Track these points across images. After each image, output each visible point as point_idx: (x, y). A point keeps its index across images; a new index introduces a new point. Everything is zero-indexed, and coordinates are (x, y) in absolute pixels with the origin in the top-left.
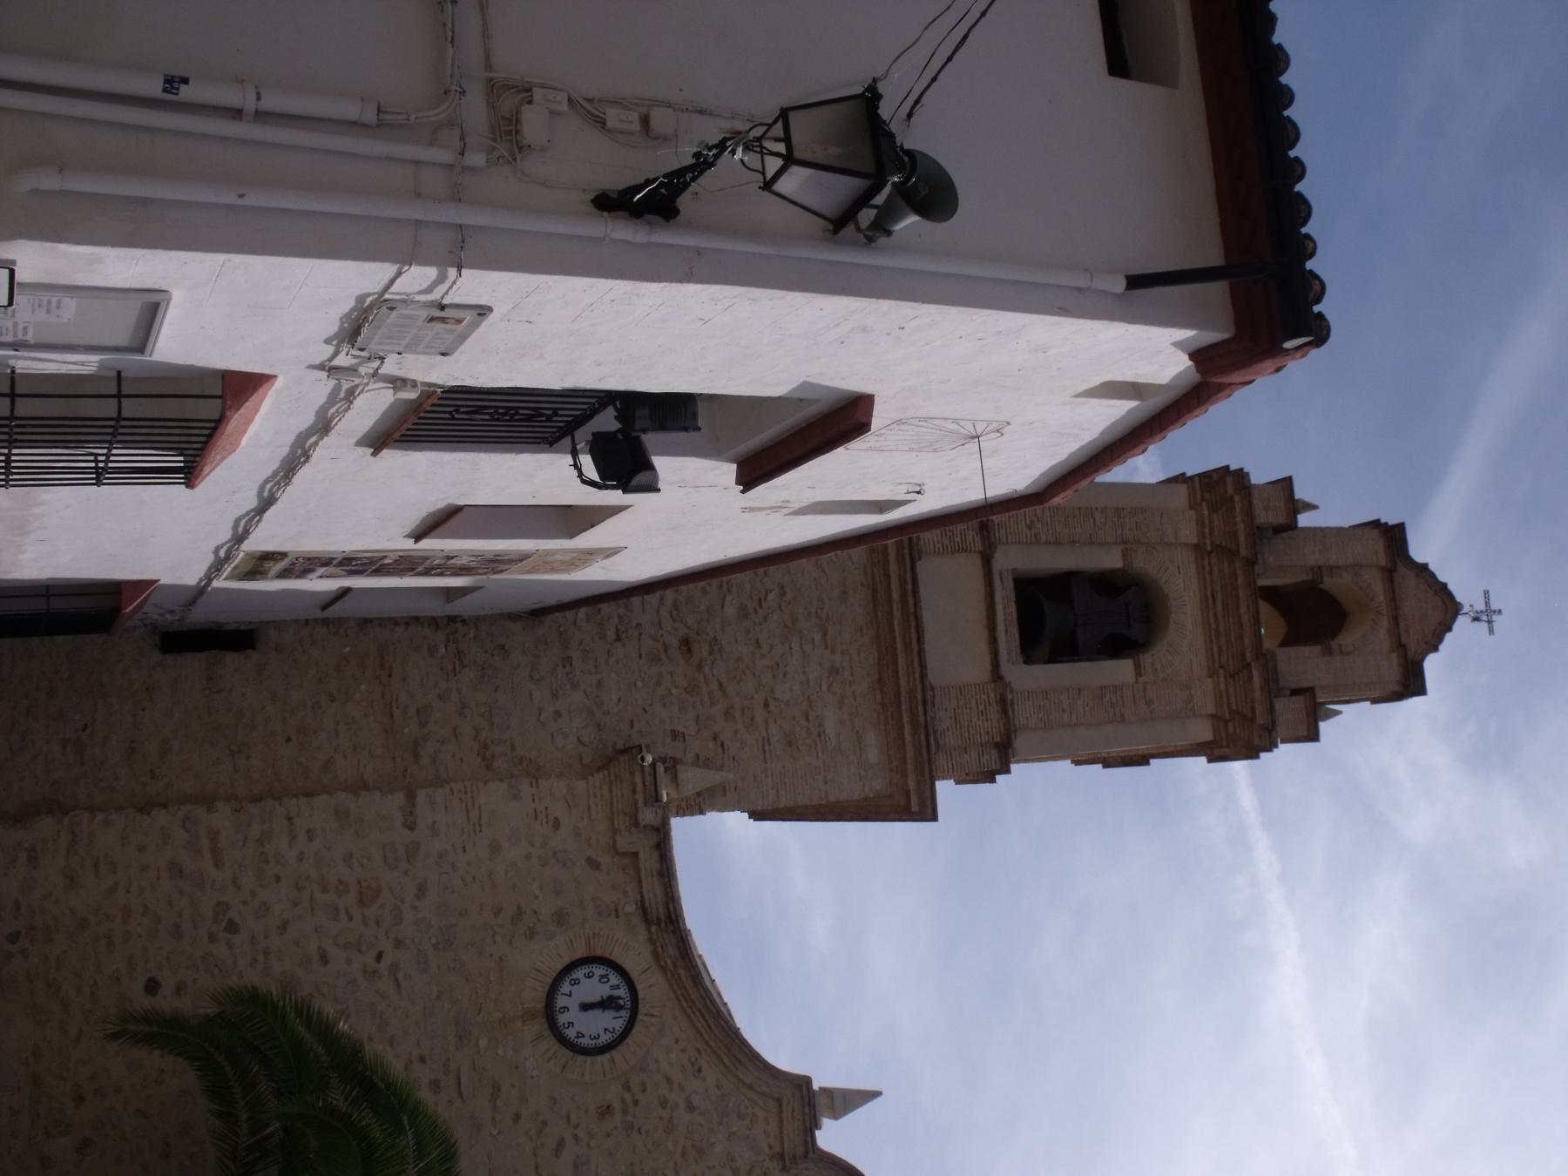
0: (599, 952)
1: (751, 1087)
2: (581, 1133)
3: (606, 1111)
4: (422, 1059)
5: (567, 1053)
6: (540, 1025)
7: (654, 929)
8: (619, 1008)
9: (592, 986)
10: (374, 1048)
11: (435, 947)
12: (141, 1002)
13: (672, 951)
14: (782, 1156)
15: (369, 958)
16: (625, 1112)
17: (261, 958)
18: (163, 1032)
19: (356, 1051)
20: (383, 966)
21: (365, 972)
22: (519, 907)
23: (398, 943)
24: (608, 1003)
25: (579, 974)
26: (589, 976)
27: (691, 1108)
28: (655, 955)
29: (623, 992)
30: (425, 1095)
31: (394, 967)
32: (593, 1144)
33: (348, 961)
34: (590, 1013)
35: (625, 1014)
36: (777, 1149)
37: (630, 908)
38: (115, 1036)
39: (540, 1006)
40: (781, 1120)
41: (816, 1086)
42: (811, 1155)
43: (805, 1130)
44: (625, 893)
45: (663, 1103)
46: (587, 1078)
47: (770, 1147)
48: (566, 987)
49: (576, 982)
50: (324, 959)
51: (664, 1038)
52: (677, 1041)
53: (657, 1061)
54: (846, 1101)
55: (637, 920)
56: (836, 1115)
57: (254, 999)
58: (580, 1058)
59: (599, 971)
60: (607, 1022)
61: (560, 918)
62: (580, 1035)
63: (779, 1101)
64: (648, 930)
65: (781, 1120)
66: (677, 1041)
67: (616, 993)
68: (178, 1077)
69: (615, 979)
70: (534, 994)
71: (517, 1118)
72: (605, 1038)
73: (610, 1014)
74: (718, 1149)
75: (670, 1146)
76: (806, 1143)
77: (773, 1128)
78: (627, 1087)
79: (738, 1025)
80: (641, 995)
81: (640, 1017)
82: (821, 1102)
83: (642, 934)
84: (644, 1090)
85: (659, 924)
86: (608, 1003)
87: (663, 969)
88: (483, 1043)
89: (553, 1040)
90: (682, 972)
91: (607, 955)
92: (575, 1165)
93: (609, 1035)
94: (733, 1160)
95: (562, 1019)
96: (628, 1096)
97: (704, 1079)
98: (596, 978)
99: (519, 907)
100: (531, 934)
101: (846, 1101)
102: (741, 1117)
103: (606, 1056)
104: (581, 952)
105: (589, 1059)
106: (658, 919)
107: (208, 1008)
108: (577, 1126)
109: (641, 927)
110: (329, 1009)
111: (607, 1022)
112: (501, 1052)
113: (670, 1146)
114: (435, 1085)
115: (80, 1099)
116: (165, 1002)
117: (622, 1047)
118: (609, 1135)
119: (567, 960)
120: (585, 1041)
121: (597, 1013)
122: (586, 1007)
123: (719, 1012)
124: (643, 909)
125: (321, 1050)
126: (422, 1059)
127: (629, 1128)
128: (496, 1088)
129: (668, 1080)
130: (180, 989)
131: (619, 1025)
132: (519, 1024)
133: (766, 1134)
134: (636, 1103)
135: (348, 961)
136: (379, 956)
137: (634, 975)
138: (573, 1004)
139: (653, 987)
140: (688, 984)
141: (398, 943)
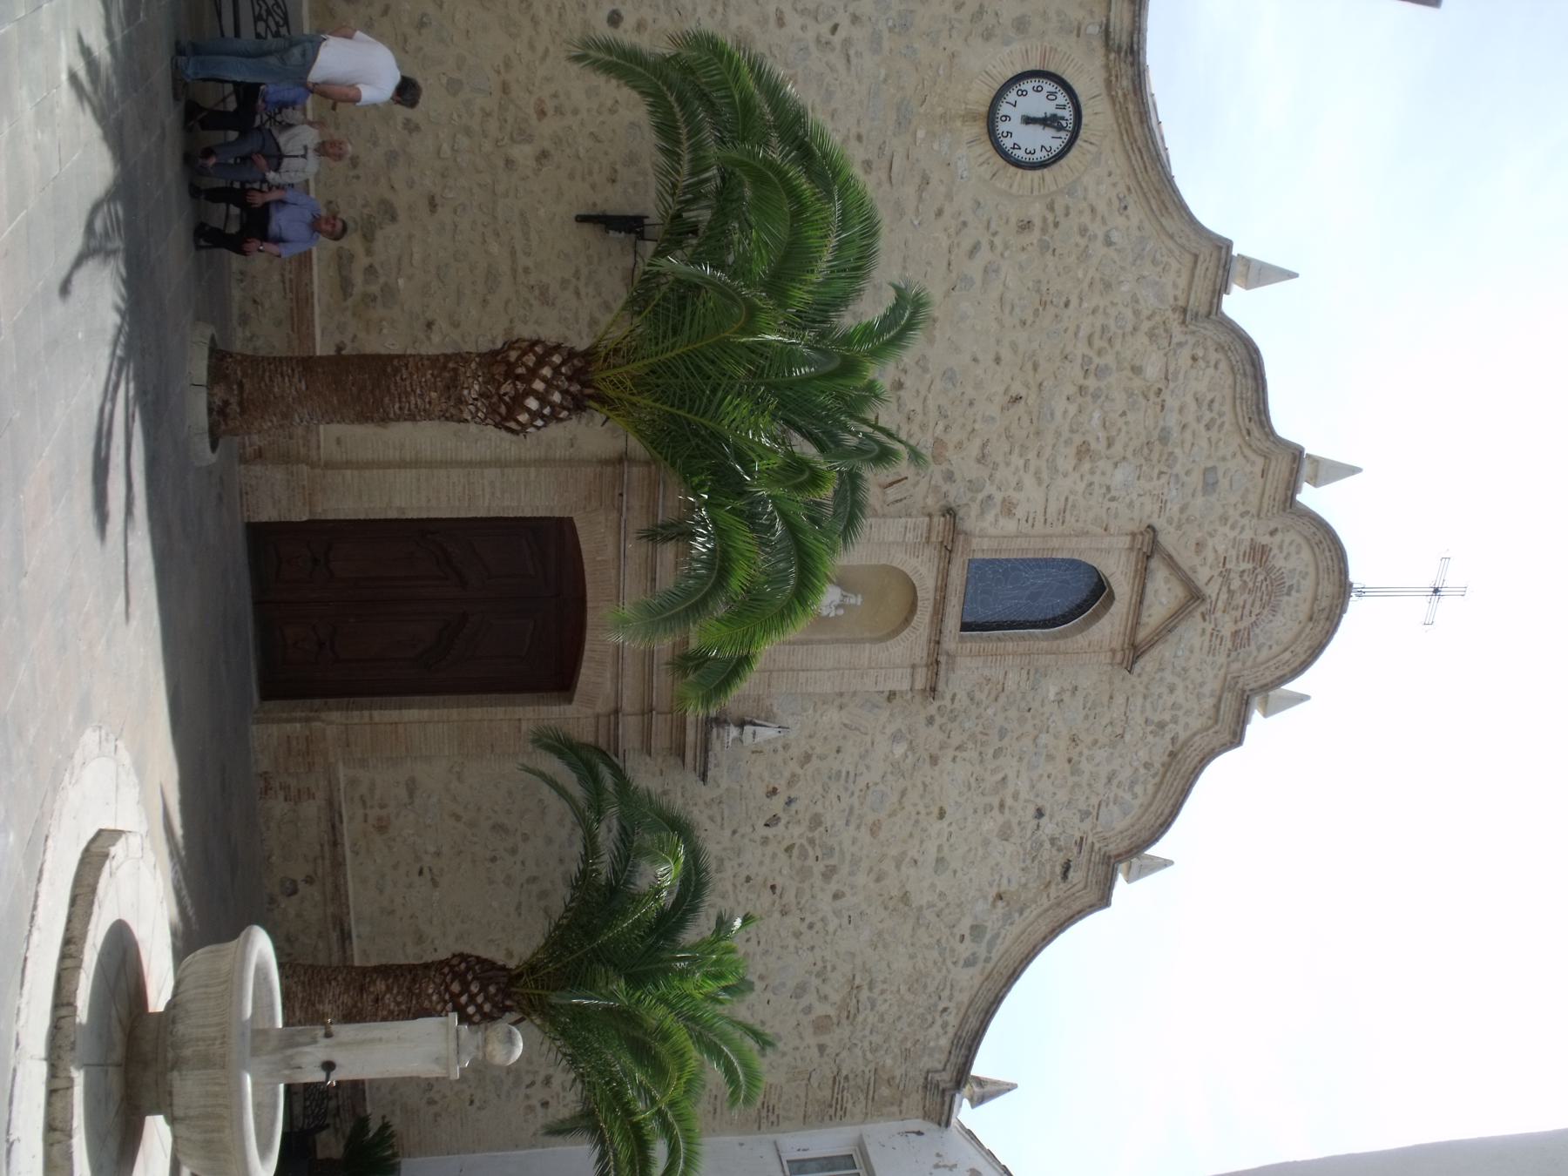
0: (1052, 69)
1: (1171, 237)
2: (998, 241)
3: (1025, 226)
4: (859, 138)
5: (1001, 162)
6: (979, 128)
7: (1112, 56)
8: (1060, 128)
9: (1037, 100)
10: (817, 116)
11: (891, 30)
12: (603, 31)
13: (1125, 83)
14: (1184, 311)
15: (825, 29)
16: (1044, 230)
17: (720, 9)
18: (621, 63)
19: (799, 117)
20: (837, 39)
21: (818, 40)
22: (981, 6)
23: (855, 19)
24: (1049, 122)
25: (1028, 85)
26: (1038, 90)
27: (1108, 242)
28: (1108, 83)
29: (1068, 113)
30: (856, 170)
31: (847, 42)
32: (1006, 254)
33: (803, 28)
34: (1031, 128)
35: (1065, 136)
36: (1181, 303)
37: (1094, 30)
38: (577, 59)
39: (984, 109)
40: (1193, 275)
41: (1235, 252)
42: (1213, 317)
43: (1214, 291)
44: (1091, 12)
45: (1083, 231)
46: (1014, 190)
47: (1176, 299)
48: (1012, 96)
49: (1023, 93)
50: (781, 22)
51: (1098, 166)
52: (1110, 174)
53: (1086, 189)
54: (1261, 274)
55: (1098, 44)
56: (1248, 286)
57: (711, 47)
58: (1012, 169)
59: (1049, 87)
60: (1039, 141)
61: (1021, 25)
62: (1016, 146)
63: (1196, 257)
64: (1107, 56)
65: (1193, 275)
66: (1110, 174)
67: (1060, 113)
68: (629, 109)
69: (1062, 98)
70: (980, 96)
71: (939, 213)
72: (1040, 156)
73: (1050, 132)
74: (1125, 288)
75: (1080, 275)
76: (1211, 304)
77: (1182, 282)
78: (1051, 208)
79: (1174, 173)
80: (1084, 120)
81: (1079, 142)
82: (1237, 268)
83: (1099, 60)
84: (1067, 215)
85: (1119, 52)
86: (1049, 122)
87: (1113, 99)
88: (921, 134)
89: (989, 146)
90: (1131, 107)
91: (1059, 73)
92: (986, 271)
93: (1044, 153)
94: (1137, 302)
95: (1002, 127)
96: (1050, 218)
97: (1128, 217)
98: (1044, 93)
99: (981, 6)
100: (988, 36)
101: (1261, 274)
102: (1154, 262)
103: (1038, 173)
104: (1034, 65)
105: (1020, 171)
106: (1120, 47)
107: (665, 49)
108: (995, 234)
109: (1100, 51)
110: (780, 71)
111: (1039, 141)
112: (936, 147)
113: (1080, 275)
114: (868, 165)
115: (542, 113)
116: (626, 36)
117: (1055, 167)
118: (1023, 249)
119: (1019, 70)
120: (1020, 154)
121: (1037, 130)
122: (1028, 120)
123: (1158, 155)
124: (1107, 33)
125: (766, 109)
126: (859, 138)
127: (1044, 247)
128: (926, 181)
129: (1093, 210)
130: (640, 26)
131: (1057, 145)
132: (959, 123)
133: (1175, 286)
134: (1056, 225)
135: (803, 28)
136: (835, 28)
137: (1082, 99)
138: (1016, 115)
139: (1098, 116)
140: (1135, 120)
141: (855, 19)
